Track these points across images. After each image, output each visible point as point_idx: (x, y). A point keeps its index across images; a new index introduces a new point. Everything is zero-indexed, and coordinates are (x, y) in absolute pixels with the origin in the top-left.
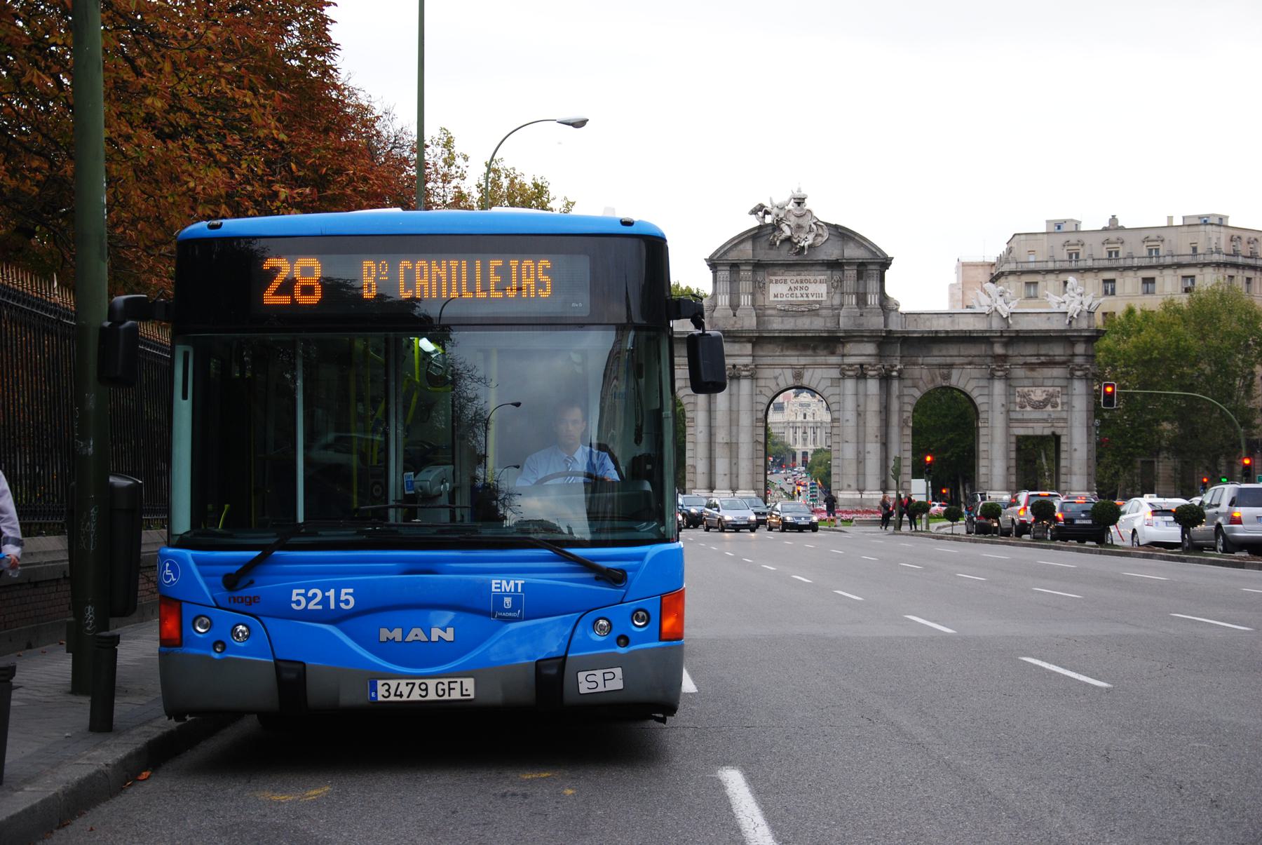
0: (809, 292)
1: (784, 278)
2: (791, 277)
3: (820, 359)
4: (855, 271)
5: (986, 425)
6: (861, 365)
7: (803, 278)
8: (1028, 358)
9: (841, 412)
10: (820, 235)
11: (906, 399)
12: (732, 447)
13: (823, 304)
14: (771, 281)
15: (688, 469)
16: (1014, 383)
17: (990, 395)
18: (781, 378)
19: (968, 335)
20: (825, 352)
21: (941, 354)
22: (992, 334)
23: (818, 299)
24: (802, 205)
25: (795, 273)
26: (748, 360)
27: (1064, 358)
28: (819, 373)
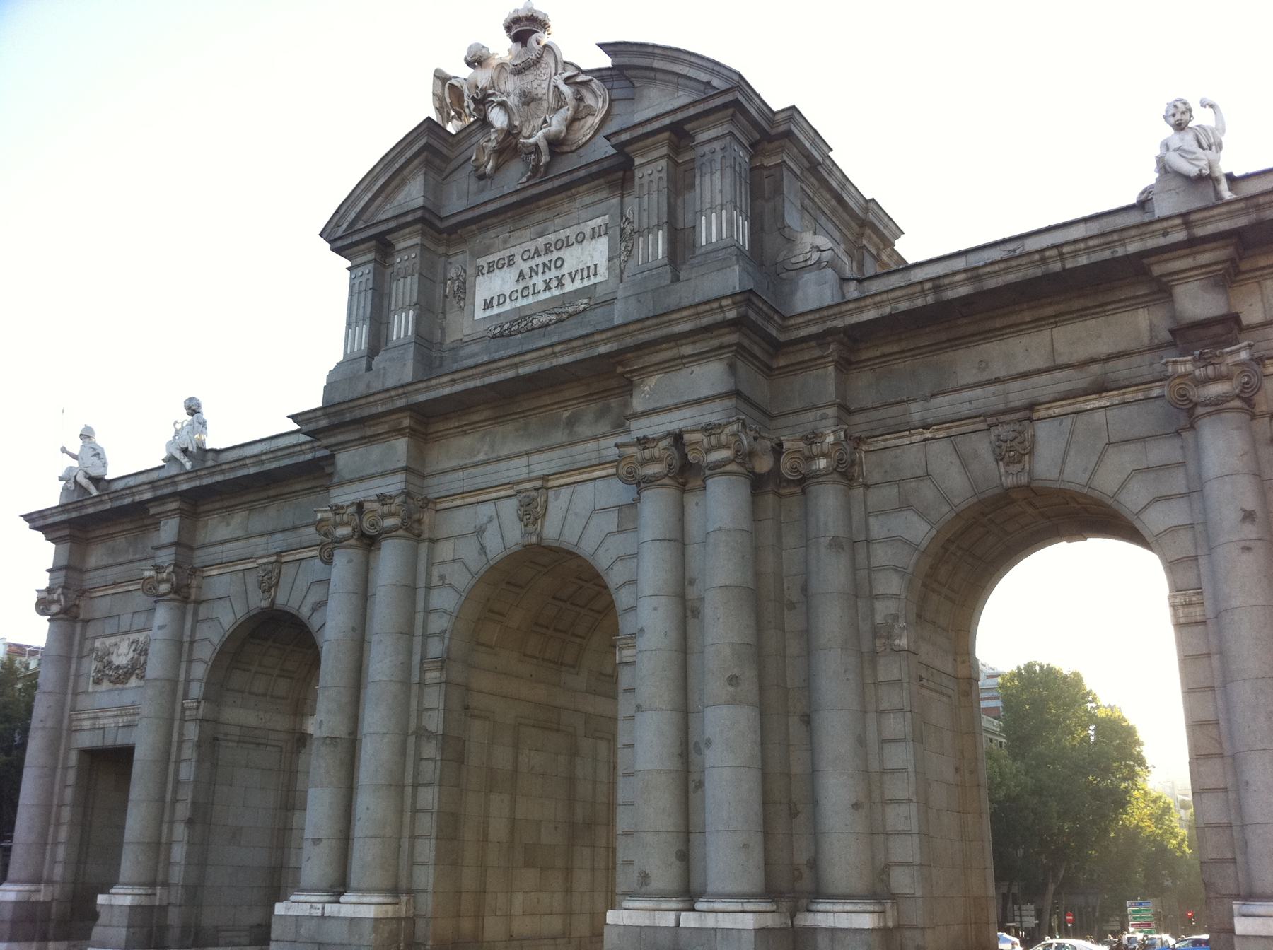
0: (565, 270)
1: (506, 253)
2: (523, 244)
3: (584, 452)
4: (663, 163)
6: (678, 438)
7: (552, 238)
10: (592, 113)
11: (882, 555)
14: (479, 272)
19: (1056, 267)
20: (603, 427)
21: (985, 376)
22: (1151, 243)
23: (586, 283)
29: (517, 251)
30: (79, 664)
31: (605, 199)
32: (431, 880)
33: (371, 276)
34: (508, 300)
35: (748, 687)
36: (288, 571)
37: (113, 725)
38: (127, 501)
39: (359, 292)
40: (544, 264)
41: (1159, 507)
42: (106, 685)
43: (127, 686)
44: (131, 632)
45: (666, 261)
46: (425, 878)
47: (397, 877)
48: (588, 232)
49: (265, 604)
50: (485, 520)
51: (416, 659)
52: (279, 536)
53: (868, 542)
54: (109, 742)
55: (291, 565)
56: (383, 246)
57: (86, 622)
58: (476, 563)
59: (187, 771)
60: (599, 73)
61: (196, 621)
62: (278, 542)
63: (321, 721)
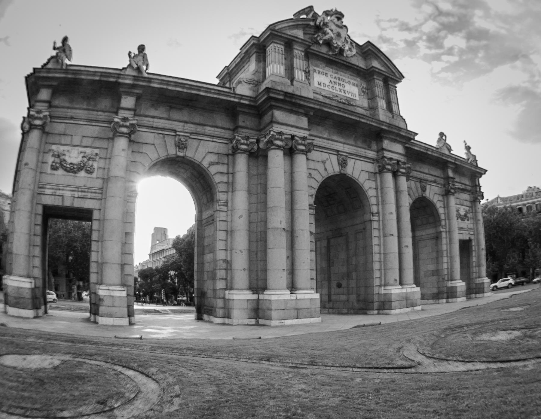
3: (361, 151)
5: (444, 230)
6: (398, 161)
7: (339, 76)
9: (380, 207)
14: (314, 71)
17: (447, 207)
18: (328, 163)
23: (352, 97)
25: (334, 71)
26: (305, 133)
27: (469, 188)
29: (329, 73)
34: (327, 87)
36: (192, 144)
37: (70, 195)
38: (112, 80)
41: (441, 208)
42: (60, 172)
43: (78, 175)
45: (386, 109)
49: (180, 154)
52: (192, 126)
54: (68, 203)
55: (195, 140)
58: (325, 175)
61: (132, 152)
62: (190, 128)
63: (281, 221)
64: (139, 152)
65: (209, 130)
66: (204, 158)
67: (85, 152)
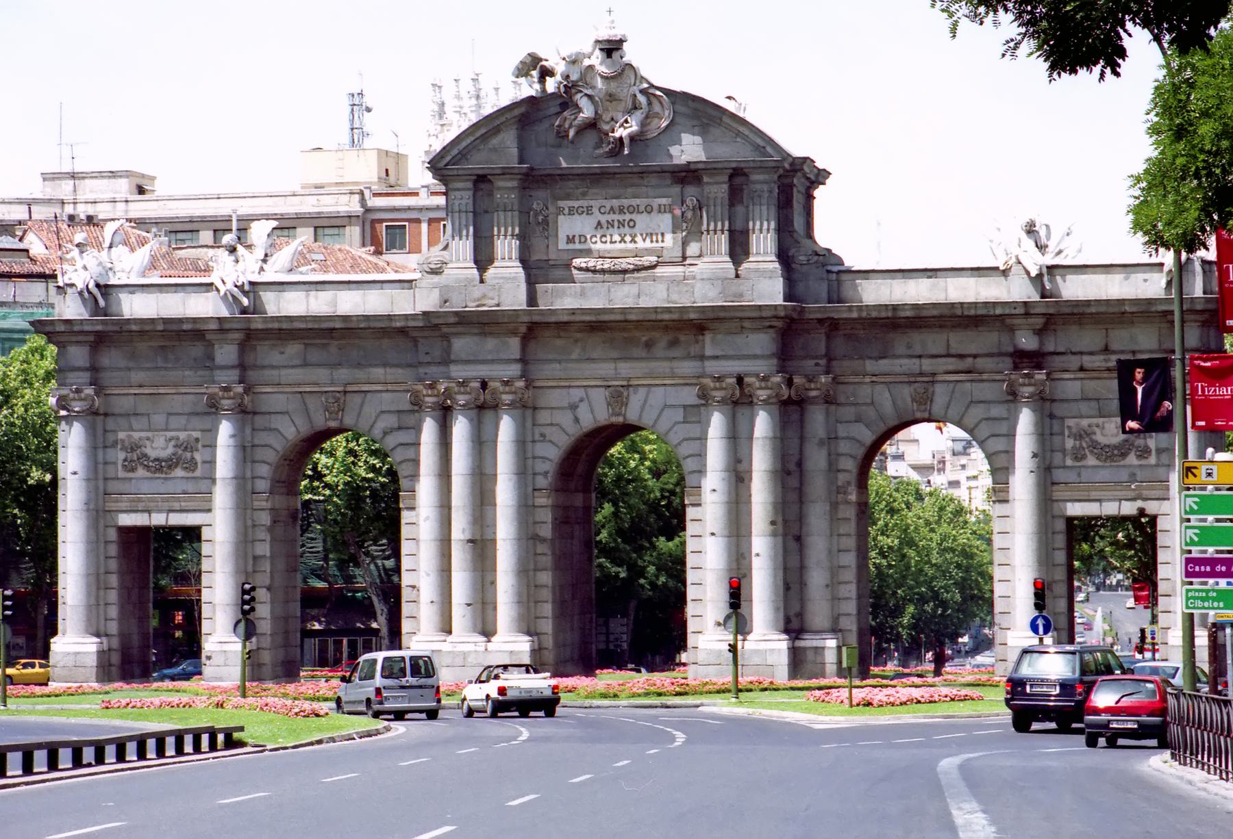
1: (584, 203)
4: (725, 187)
7: (626, 202)
8: (1086, 358)
11: (844, 447)
12: (482, 548)
13: (665, 251)
14: (560, 211)
15: (406, 594)
16: (1059, 409)
21: (910, 352)
23: (655, 245)
24: (616, 55)
25: (611, 192)
28: (658, 396)
30: (104, 454)
31: (668, 186)
32: (550, 627)
33: (471, 201)
35: (780, 527)
39: (460, 211)
40: (619, 221)
42: (141, 472)
43: (172, 475)
44: (166, 430)
45: (728, 259)
46: (547, 626)
47: (528, 628)
48: (655, 207)
50: (577, 399)
51: (530, 489)
53: (836, 438)
56: (481, 181)
57: (106, 415)
59: (264, 549)
60: (668, 92)
61: (253, 429)
62: (343, 374)
63: (464, 530)
64: (265, 429)
65: (378, 372)
66: (374, 423)
67: (178, 439)
